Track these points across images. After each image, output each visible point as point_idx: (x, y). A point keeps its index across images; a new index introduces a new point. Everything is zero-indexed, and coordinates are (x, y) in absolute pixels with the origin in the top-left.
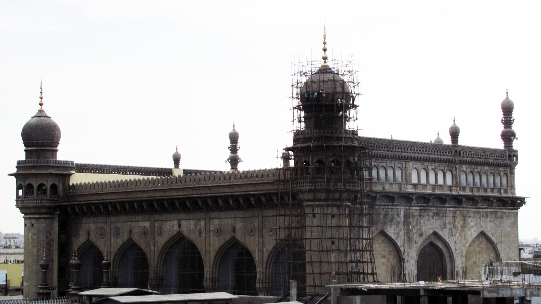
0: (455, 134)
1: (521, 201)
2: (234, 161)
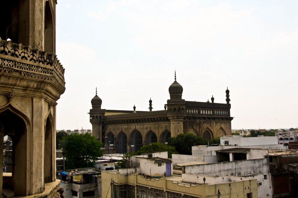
0: (213, 99)
1: (232, 118)
2: (151, 108)
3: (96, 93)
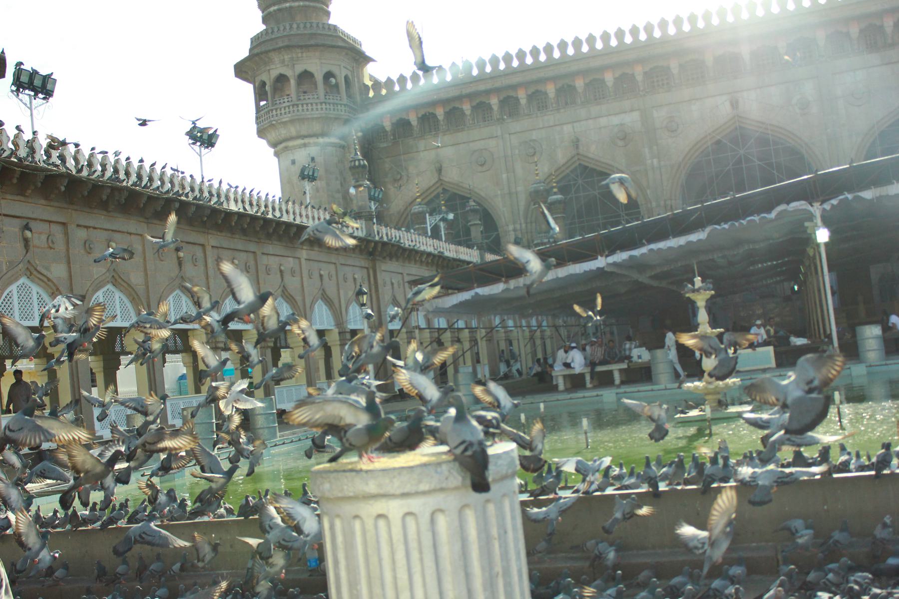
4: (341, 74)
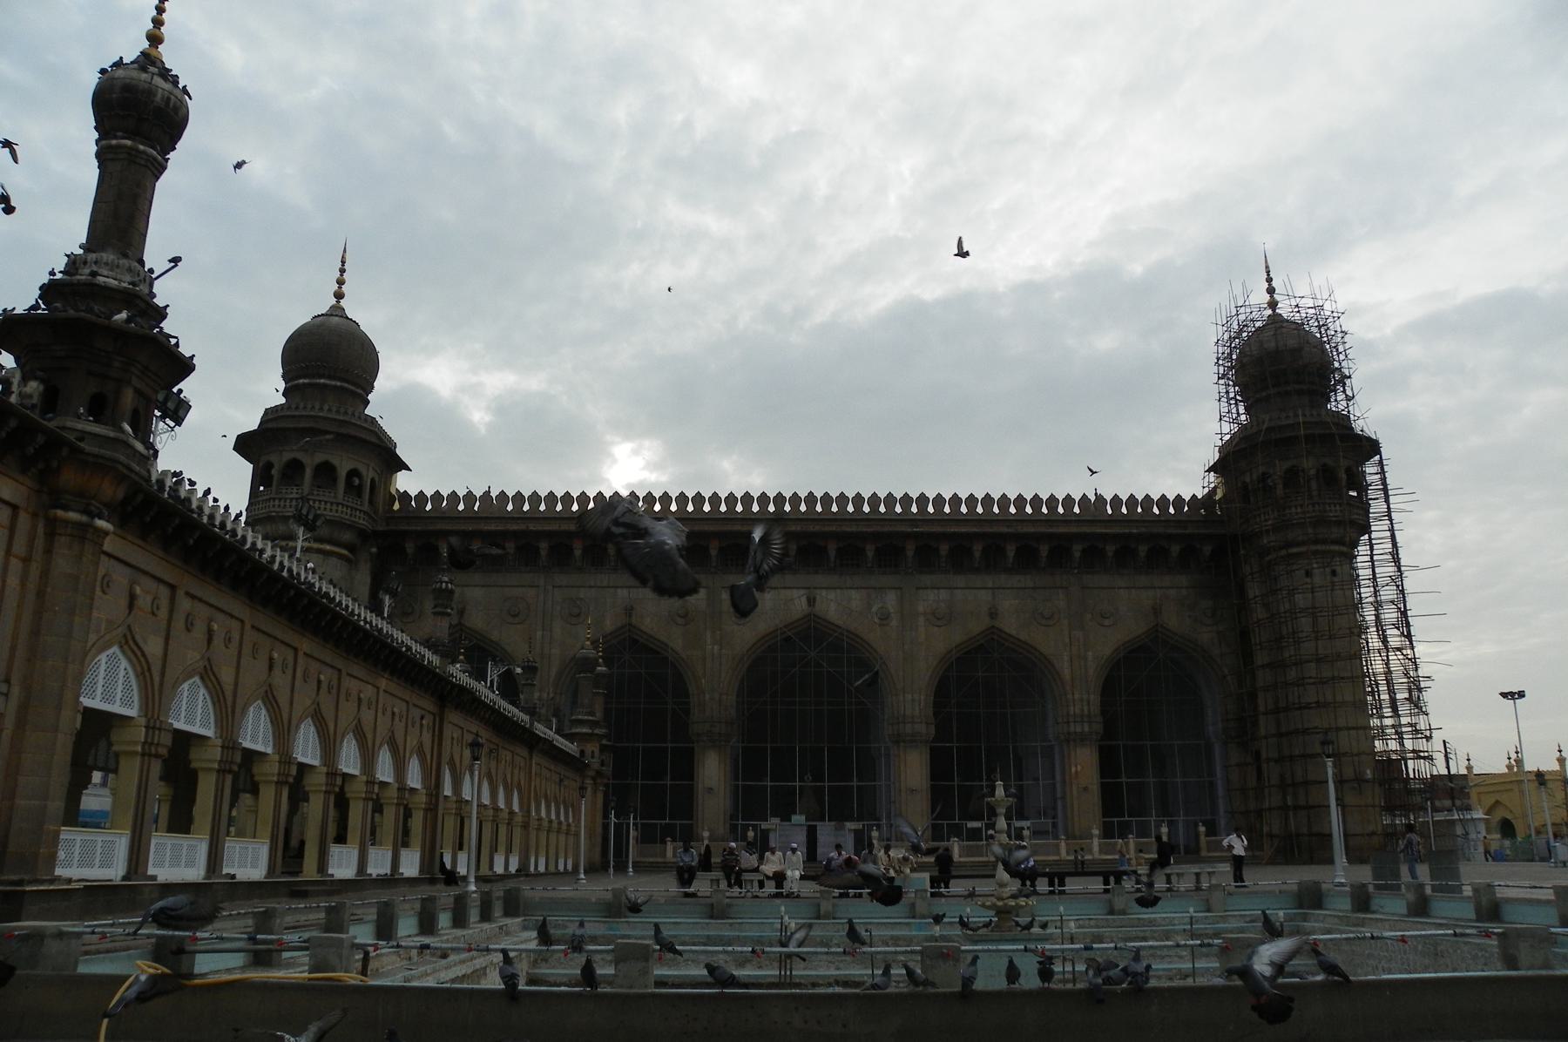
3: (339, 296)
4: (369, 474)
